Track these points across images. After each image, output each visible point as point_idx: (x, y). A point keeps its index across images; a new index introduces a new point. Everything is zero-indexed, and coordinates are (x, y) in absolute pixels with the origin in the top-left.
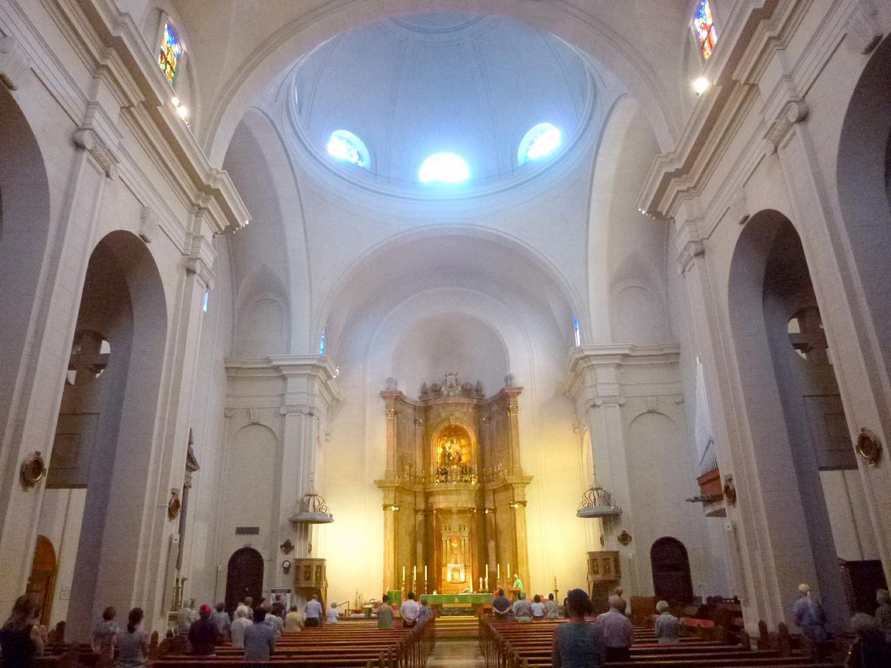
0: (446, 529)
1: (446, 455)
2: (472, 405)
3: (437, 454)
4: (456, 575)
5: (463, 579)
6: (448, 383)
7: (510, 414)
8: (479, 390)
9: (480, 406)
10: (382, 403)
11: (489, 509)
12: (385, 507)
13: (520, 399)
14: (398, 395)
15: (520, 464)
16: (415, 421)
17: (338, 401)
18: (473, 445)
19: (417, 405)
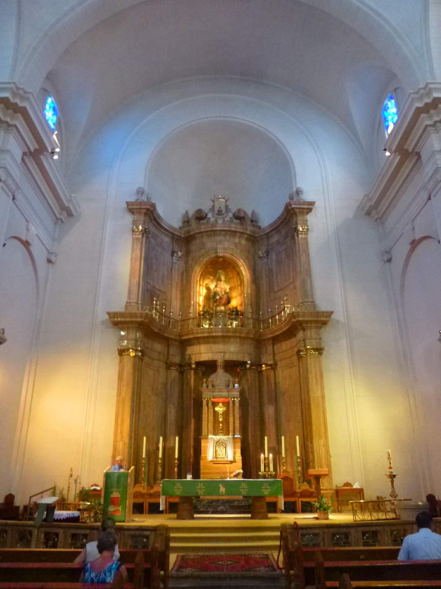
0: (207, 387)
1: (211, 297)
2: (245, 236)
3: (200, 295)
4: (221, 451)
5: (230, 458)
6: (216, 209)
7: (298, 236)
8: (254, 221)
9: (255, 237)
10: (129, 218)
11: (267, 365)
12: (122, 352)
13: (310, 218)
14: (148, 207)
15: (312, 297)
16: (173, 253)
17: (70, 214)
18: (246, 282)
19: (176, 233)
